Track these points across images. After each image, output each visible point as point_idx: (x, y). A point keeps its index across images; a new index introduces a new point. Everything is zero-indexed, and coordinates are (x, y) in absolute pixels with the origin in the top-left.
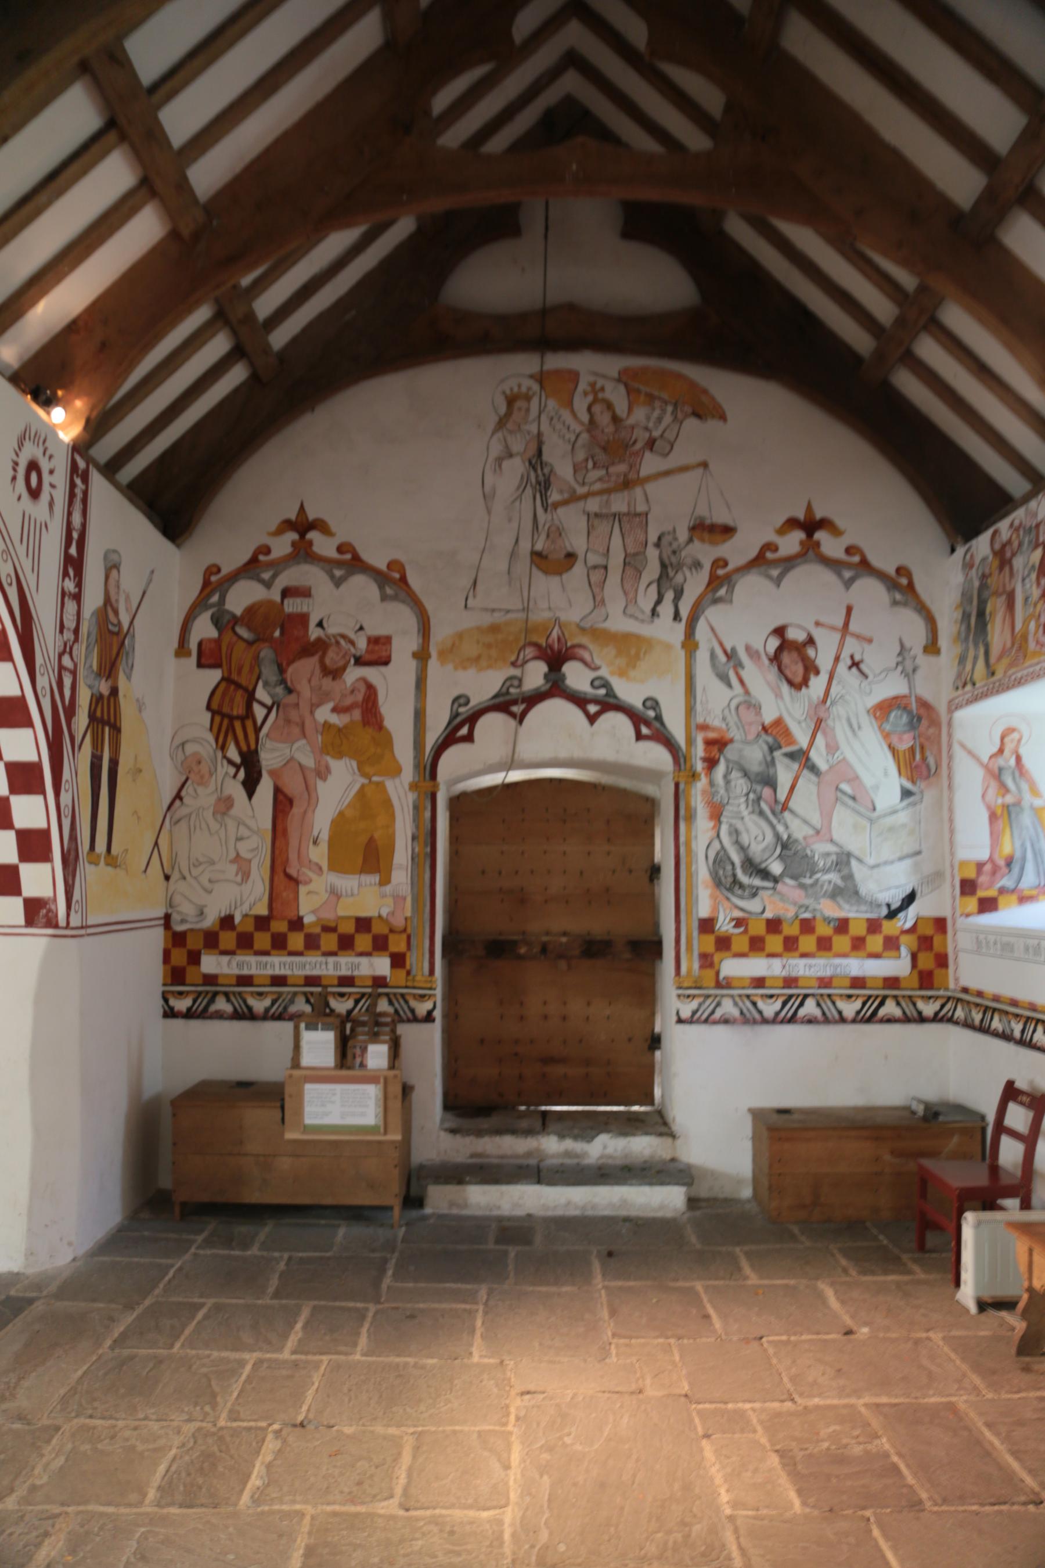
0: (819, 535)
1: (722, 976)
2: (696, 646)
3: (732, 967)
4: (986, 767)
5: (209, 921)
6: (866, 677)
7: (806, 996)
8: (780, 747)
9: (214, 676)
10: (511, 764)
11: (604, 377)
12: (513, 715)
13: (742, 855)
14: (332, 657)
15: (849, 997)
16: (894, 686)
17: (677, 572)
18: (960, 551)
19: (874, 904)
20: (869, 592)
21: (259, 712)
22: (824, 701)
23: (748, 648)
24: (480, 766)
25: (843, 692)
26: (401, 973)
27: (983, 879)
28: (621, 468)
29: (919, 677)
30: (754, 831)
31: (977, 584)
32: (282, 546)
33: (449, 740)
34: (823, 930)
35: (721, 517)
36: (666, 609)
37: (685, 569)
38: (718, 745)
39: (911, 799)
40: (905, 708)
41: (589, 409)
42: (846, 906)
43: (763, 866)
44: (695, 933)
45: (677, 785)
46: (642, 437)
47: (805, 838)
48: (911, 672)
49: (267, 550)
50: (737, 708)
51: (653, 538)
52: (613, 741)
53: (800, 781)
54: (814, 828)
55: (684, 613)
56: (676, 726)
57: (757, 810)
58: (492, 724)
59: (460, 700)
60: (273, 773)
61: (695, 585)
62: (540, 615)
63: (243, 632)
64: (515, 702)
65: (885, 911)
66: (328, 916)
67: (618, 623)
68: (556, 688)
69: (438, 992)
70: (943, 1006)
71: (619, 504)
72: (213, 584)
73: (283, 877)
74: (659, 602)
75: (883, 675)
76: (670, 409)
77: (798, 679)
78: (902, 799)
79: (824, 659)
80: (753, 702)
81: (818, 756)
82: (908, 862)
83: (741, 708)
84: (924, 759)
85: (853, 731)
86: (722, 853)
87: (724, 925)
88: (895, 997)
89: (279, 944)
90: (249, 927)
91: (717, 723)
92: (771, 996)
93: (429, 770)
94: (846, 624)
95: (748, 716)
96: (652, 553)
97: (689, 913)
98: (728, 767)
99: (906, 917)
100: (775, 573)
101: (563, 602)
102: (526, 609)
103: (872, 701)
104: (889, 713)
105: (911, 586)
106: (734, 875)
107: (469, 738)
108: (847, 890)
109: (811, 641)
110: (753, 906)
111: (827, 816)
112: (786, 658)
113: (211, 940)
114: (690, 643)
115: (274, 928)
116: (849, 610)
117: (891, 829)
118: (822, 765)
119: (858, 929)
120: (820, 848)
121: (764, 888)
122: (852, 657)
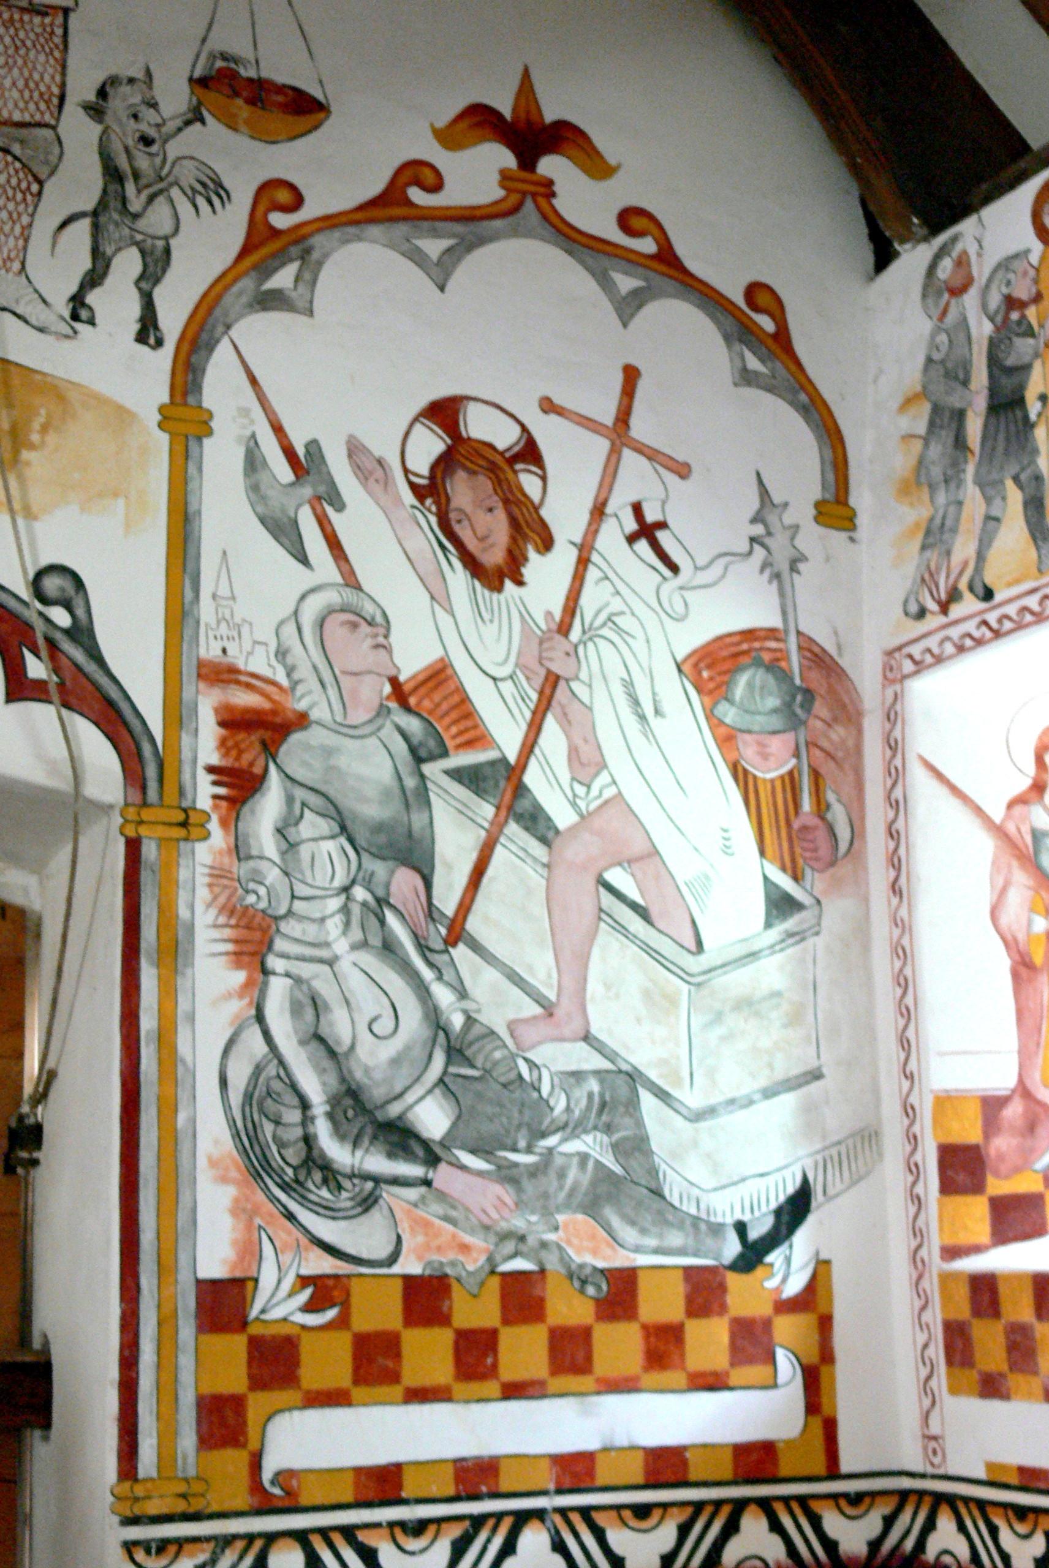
0: (550, 165)
1: (270, 1466)
2: (203, 426)
3: (306, 1440)
4: (998, 831)
6: (674, 568)
7: (522, 1518)
8: (445, 754)
13: (332, 1080)
15: (642, 1511)
16: (736, 605)
17: (151, 199)
18: (913, 259)
19: (704, 1227)
20: (679, 339)
22: (564, 629)
23: (354, 449)
25: (616, 605)
27: (1002, 1145)
29: (804, 583)
30: (369, 1003)
31: (982, 329)
34: (569, 1308)
35: (284, 67)
36: (116, 303)
37: (175, 192)
38: (261, 730)
39: (790, 924)
40: (775, 667)
42: (629, 1234)
43: (394, 1110)
44: (187, 1330)
45: (133, 847)
47: (512, 1027)
48: (784, 567)
50: (321, 624)
51: (82, 86)
53: (500, 854)
54: (539, 999)
55: (172, 320)
57: (376, 941)
61: (206, 246)
65: (732, 1248)
70: (889, 1522)
74: (94, 279)
75: (717, 569)
77: (494, 557)
78: (768, 925)
79: (564, 508)
80: (369, 609)
81: (548, 785)
82: (788, 1101)
83: (334, 624)
84: (821, 808)
85: (642, 718)
86: (272, 1070)
87: (277, 1302)
88: (765, 1505)
91: (260, 663)
92: (418, 1528)
94: (624, 417)
95: (354, 651)
96: (79, 133)
97: (166, 1269)
98: (290, 800)
99: (788, 1260)
100: (434, 247)
103: (693, 636)
104: (734, 671)
105: (782, 340)
106: (308, 1140)
108: (631, 1185)
109: (529, 452)
110: (367, 1237)
111: (575, 963)
112: (463, 491)
114: (185, 417)
116: (631, 375)
117: (745, 1004)
118: (562, 816)
119: (661, 1303)
120: (556, 1056)
121: (396, 1181)
122: (637, 509)
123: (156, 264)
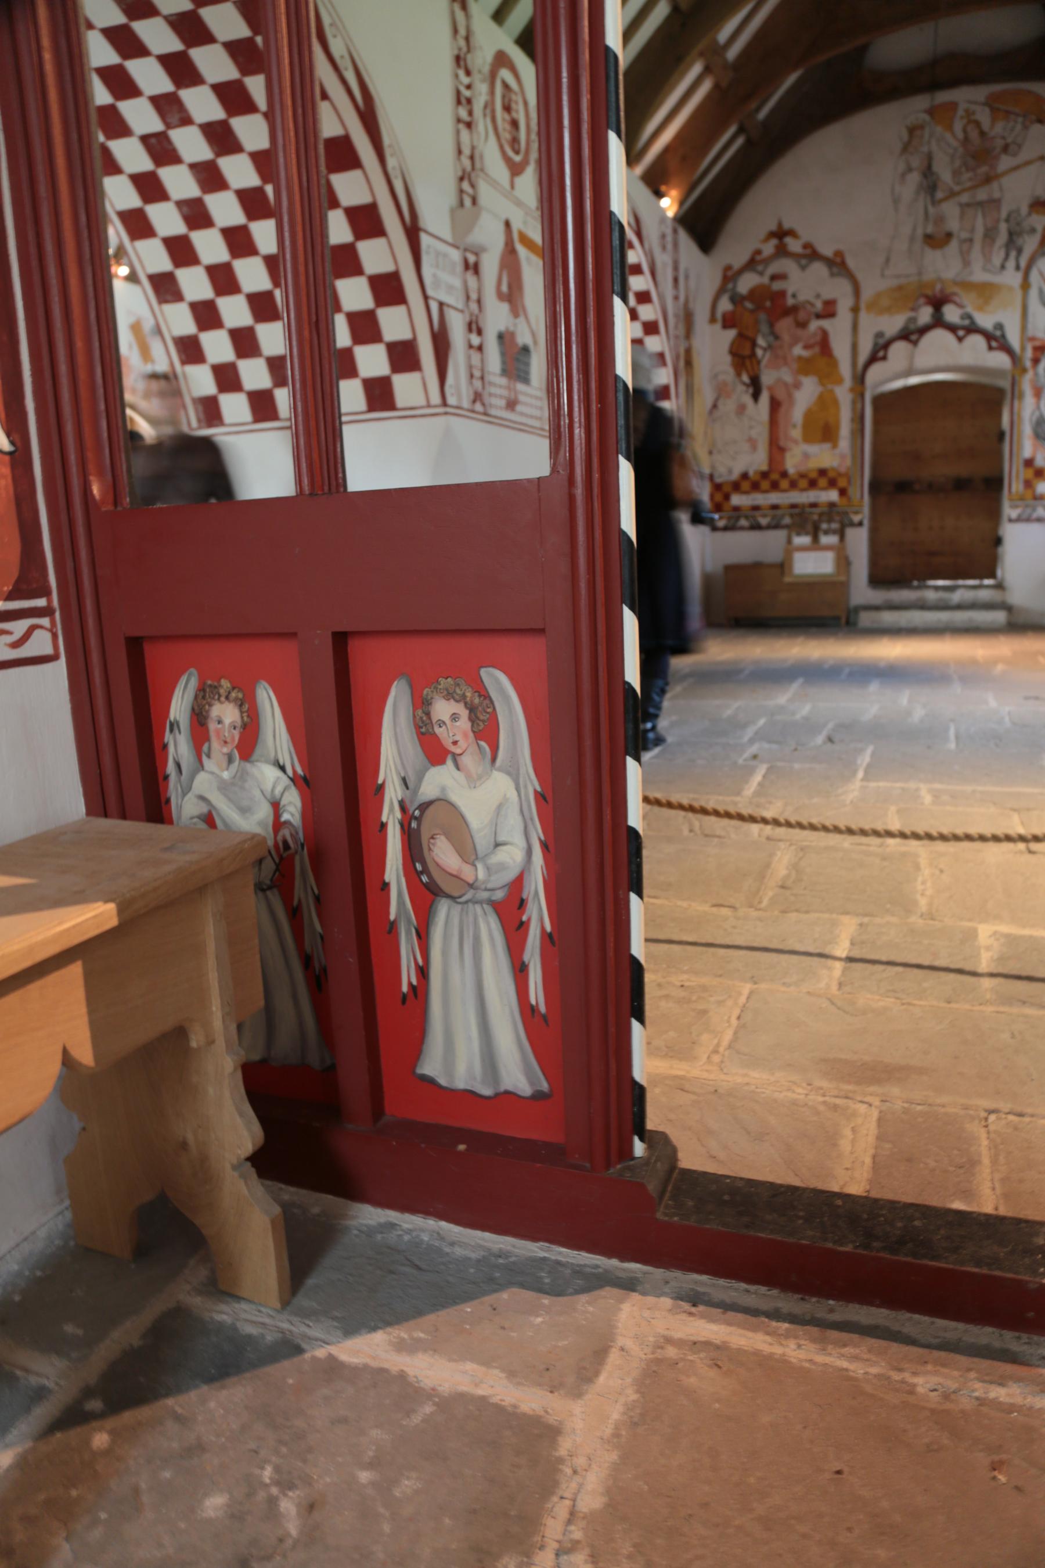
5: (735, 476)
9: (731, 334)
10: (910, 372)
11: (975, 103)
12: (911, 341)
14: (802, 315)
21: (759, 352)
24: (893, 376)
26: (844, 501)
28: (983, 170)
32: (769, 249)
33: (873, 359)
36: (1011, 264)
41: (965, 131)
46: (999, 143)
49: (758, 252)
51: (1004, 214)
52: (975, 353)
55: (1023, 263)
56: (1014, 339)
58: (899, 350)
59: (879, 335)
60: (770, 388)
61: (1030, 244)
62: (929, 276)
63: (749, 305)
64: (912, 333)
66: (803, 469)
67: (979, 275)
68: (938, 322)
69: (866, 510)
71: (982, 195)
72: (729, 277)
73: (776, 448)
76: (1020, 119)
89: (775, 486)
90: (757, 478)
93: (860, 379)
101: (943, 266)
102: (920, 274)
107: (884, 358)
113: (736, 487)
114: (1026, 285)
115: (772, 478)
123: (1020, 251)
